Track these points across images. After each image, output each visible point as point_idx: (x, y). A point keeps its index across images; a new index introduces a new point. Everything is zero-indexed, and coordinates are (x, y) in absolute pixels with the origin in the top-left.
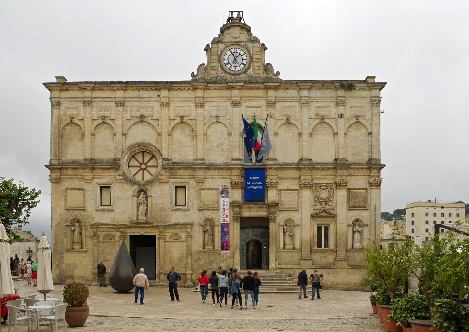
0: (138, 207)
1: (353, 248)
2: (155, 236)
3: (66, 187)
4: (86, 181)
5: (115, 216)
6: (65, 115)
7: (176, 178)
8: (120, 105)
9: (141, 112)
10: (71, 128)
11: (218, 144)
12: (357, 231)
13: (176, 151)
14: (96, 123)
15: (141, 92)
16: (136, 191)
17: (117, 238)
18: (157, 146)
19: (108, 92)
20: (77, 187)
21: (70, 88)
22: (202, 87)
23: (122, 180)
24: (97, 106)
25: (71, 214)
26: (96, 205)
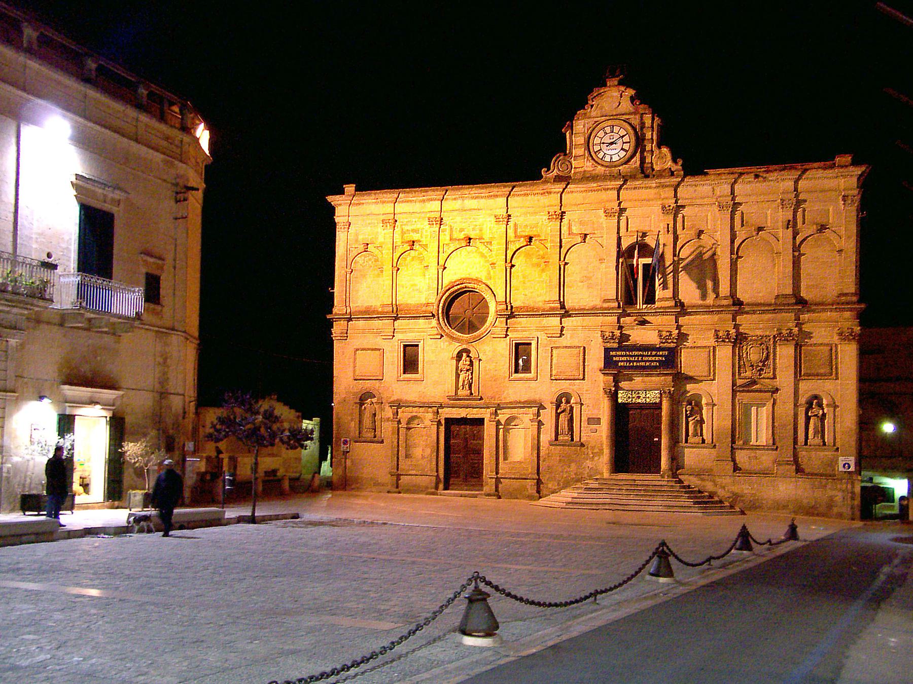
0: (458, 376)
1: (806, 444)
2: (484, 419)
3: (355, 347)
4: (384, 337)
5: (425, 388)
6: (357, 240)
7: (517, 331)
8: (434, 223)
9: (466, 233)
10: (364, 260)
11: (583, 277)
12: (814, 416)
13: (518, 290)
14: (400, 251)
15: (466, 202)
16: (456, 352)
17: (427, 423)
18: (488, 283)
19: (418, 205)
20: (370, 347)
21: (364, 201)
22: (557, 190)
23: (437, 334)
24: (401, 225)
25: (361, 386)
26: (398, 373)
